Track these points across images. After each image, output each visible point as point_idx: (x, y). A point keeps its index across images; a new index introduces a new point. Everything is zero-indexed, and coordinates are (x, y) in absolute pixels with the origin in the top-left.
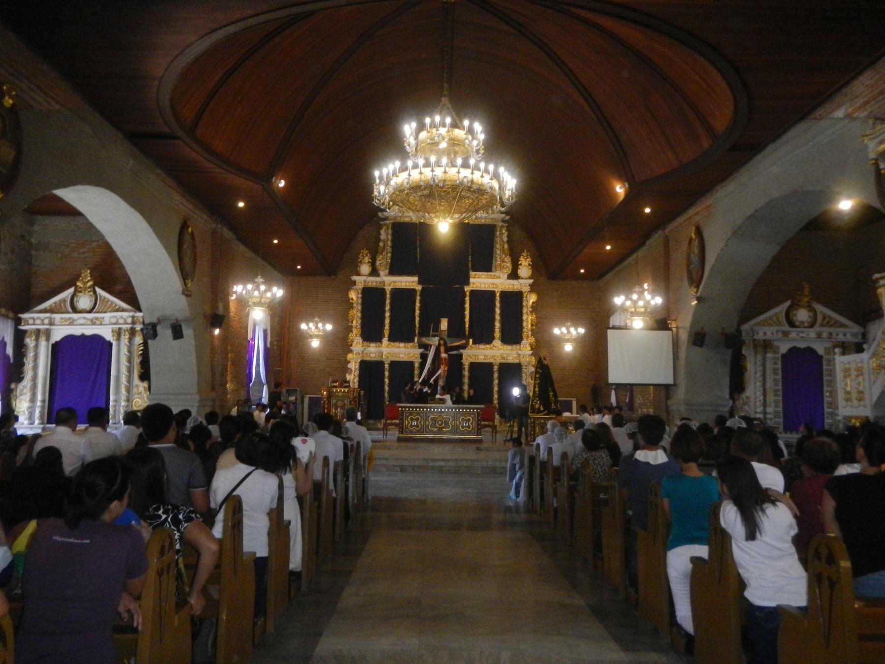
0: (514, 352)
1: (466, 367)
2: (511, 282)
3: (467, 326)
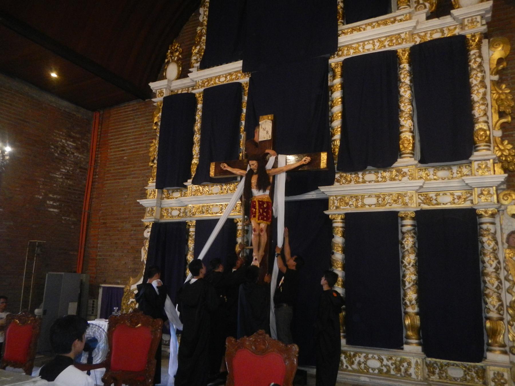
0: (455, 183)
1: (338, 224)
2: (435, 22)
3: (337, 136)
